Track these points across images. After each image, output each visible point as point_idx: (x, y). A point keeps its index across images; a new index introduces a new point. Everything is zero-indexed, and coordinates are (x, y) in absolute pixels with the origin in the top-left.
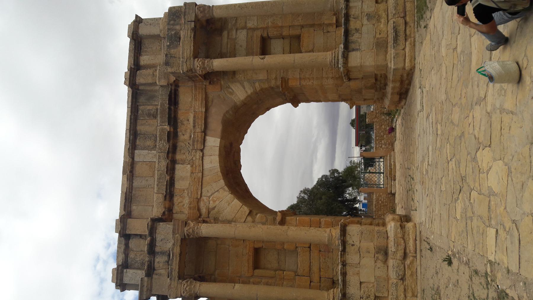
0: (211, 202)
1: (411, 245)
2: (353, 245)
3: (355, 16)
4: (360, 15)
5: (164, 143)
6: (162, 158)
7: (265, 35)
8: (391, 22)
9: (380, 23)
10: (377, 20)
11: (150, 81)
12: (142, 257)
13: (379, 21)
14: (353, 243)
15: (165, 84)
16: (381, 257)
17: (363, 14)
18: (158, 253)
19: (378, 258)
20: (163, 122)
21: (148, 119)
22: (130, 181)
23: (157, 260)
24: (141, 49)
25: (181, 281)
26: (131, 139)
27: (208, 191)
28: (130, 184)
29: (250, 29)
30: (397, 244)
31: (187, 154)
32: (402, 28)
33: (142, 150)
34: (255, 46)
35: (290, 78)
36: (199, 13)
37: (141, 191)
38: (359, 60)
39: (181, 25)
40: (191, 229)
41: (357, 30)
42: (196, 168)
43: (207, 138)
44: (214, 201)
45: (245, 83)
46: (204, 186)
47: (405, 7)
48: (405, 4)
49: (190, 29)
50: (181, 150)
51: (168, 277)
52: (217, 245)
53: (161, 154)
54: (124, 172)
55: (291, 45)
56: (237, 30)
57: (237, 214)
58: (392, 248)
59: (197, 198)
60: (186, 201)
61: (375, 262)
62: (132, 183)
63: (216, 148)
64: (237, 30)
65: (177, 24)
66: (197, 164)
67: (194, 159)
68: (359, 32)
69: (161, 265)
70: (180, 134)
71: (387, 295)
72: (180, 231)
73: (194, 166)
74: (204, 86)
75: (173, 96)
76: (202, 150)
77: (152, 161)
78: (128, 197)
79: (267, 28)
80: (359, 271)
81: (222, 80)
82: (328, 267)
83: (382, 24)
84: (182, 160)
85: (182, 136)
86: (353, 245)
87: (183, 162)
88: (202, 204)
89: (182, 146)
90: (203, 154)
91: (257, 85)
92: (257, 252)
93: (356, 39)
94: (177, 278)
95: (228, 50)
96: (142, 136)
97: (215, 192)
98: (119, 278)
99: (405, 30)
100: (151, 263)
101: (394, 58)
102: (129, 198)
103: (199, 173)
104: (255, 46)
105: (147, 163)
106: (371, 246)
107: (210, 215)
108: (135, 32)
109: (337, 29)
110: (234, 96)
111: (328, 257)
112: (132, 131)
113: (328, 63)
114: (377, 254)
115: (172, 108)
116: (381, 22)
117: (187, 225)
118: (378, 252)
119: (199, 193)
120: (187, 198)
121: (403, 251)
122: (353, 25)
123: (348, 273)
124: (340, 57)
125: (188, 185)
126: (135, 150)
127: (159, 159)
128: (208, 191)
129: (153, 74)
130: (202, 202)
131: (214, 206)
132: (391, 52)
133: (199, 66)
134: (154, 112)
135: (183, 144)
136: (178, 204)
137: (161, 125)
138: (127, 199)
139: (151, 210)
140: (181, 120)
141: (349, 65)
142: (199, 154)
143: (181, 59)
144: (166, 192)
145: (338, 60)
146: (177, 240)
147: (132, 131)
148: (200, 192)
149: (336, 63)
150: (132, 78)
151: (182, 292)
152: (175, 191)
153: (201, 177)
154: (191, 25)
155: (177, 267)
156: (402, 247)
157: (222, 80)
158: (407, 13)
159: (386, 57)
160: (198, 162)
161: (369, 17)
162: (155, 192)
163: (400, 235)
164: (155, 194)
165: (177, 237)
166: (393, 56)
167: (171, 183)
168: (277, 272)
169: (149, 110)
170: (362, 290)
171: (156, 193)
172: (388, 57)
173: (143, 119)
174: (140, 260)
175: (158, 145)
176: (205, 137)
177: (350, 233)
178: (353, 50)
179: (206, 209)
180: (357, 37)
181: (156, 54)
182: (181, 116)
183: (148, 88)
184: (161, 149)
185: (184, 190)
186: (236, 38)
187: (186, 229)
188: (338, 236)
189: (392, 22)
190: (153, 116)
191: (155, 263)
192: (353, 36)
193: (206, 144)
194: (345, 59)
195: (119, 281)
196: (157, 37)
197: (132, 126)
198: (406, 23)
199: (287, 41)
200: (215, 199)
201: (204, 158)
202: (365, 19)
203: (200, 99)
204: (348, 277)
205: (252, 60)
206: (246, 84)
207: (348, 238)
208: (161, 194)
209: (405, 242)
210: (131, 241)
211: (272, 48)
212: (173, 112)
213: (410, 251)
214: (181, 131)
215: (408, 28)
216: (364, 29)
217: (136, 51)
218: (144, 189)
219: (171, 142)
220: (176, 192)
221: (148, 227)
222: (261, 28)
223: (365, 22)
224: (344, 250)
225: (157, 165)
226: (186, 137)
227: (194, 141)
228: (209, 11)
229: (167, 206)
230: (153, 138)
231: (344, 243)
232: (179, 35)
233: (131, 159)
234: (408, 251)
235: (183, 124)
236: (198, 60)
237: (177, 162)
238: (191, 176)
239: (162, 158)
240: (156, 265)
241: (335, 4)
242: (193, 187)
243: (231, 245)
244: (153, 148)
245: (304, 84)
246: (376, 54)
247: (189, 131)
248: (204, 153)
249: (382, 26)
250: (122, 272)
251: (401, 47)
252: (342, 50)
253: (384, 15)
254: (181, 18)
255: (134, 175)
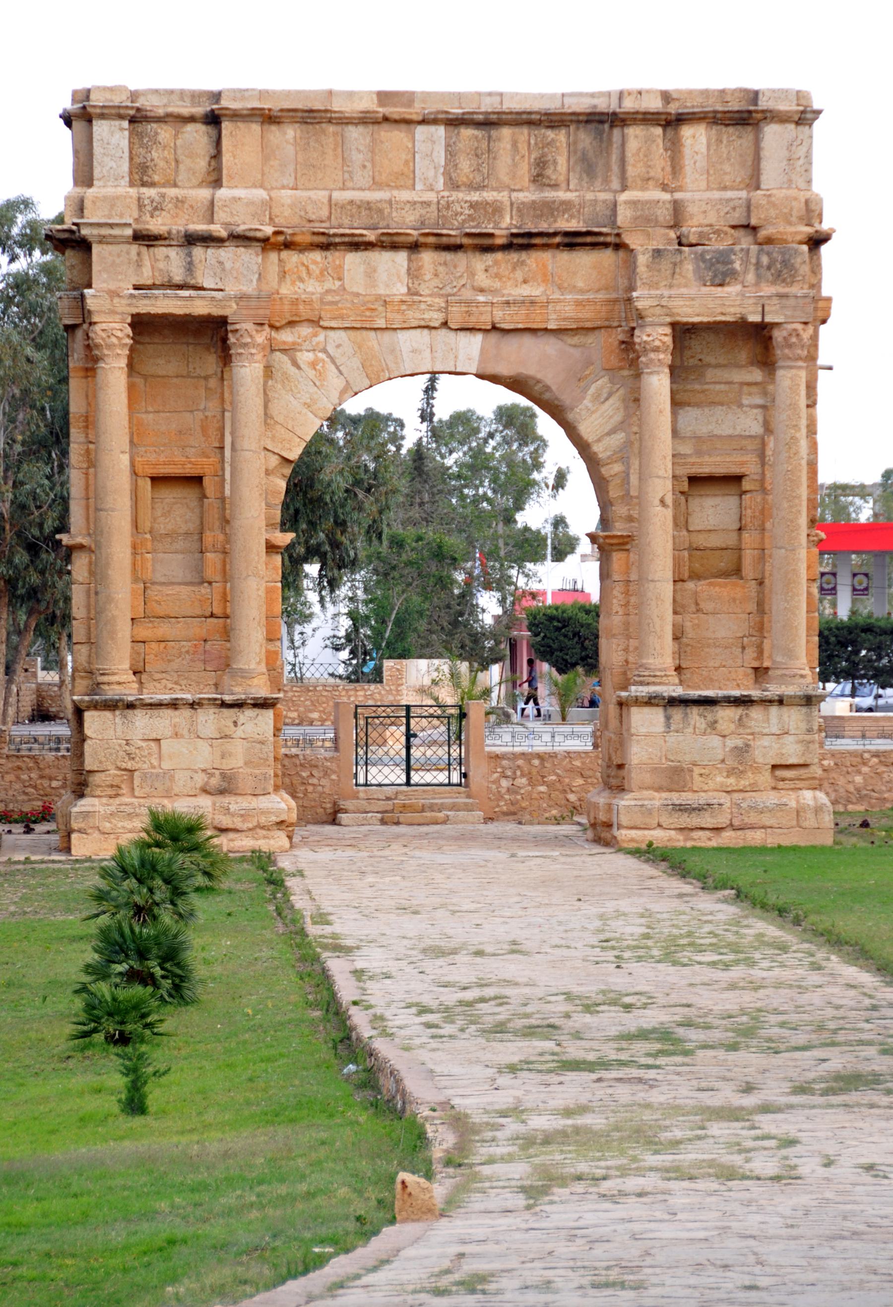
0: (311, 356)
1: (244, 843)
2: (235, 723)
3: (745, 720)
4: (749, 731)
5: (463, 217)
6: (423, 212)
7: (746, 485)
8: (725, 799)
9: (725, 774)
10: (734, 769)
11: (631, 171)
12: (162, 164)
13: (731, 772)
14: (239, 724)
15: (620, 220)
16: (215, 782)
17: (750, 737)
18: (189, 255)
19: (212, 775)
20: (519, 210)
21: (529, 158)
22: (360, 118)
23: (173, 253)
24: (727, 125)
25: (129, 320)
26: (475, 116)
27: (338, 346)
28: (354, 118)
29: (764, 444)
30: (245, 816)
31: (436, 282)
32: (707, 820)
33: (448, 145)
34: (718, 459)
35: (631, 555)
36: (785, 333)
37: (335, 150)
38: (643, 730)
39: (757, 284)
40: (249, 340)
41: (713, 725)
42: (398, 311)
43: (479, 337)
44: (313, 365)
45: (623, 434)
46: (350, 332)
47: (752, 828)
48: (762, 828)
49: (744, 311)
50: (445, 264)
51: (136, 288)
52: (206, 378)
53: (434, 207)
54: (384, 97)
55: (722, 549)
56: (764, 407)
57: (283, 430)
58: (236, 804)
59: (320, 318)
60: (312, 288)
61: (203, 771)
62: (356, 124)
63: (452, 363)
64: (764, 407)
65: (759, 277)
66: (410, 314)
67: (423, 306)
68: (709, 730)
69: (161, 265)
70: (490, 258)
71: (136, 794)
72: (244, 312)
73: (404, 307)
74: (616, 324)
75: (589, 239)
76: (445, 324)
77: (417, 180)
78: (315, 114)
79: (764, 490)
80: (182, 736)
81: (632, 372)
82: (169, 661)
83: (722, 779)
84: (420, 268)
85: (483, 267)
86: (235, 723)
87: (413, 273)
88: (305, 330)
89: (455, 267)
90: (435, 328)
91: (617, 468)
92: (196, 480)
93: (693, 723)
94: (135, 311)
95: (711, 387)
96: (484, 145)
97: (337, 368)
98: (106, 111)
99: (702, 829)
100: (165, 239)
101: (642, 806)
102: (315, 118)
103: (383, 321)
104: (718, 459)
105: (411, 164)
106: (236, 762)
107: (278, 353)
108: (768, 115)
109: (750, 671)
110: (590, 405)
111: (192, 660)
112: (495, 116)
113: (644, 661)
114: (221, 774)
115: (558, 239)
116: (728, 777)
117: (259, 328)
118: (224, 776)
119: (333, 324)
120: (319, 290)
121: (231, 826)
122: (726, 715)
123: (177, 713)
124: (652, 689)
125: (355, 290)
126: (446, 124)
127: (422, 203)
128: (338, 346)
129: (649, 179)
130: (310, 330)
131: (302, 366)
132: (657, 799)
133: (651, 338)
134: (548, 177)
135: (461, 268)
136: (303, 264)
137: (512, 204)
138: (311, 115)
139: (285, 182)
140: (524, 261)
141: (634, 710)
142: (436, 318)
143: (666, 293)
144: (335, 235)
145: (648, 684)
146: (223, 307)
147: (495, 116)
148: (335, 326)
149: (642, 679)
150: (640, 116)
151: (104, 326)
152: (337, 254)
153: (376, 326)
154: (754, 313)
155: (160, 311)
156: (238, 823)
157: (632, 372)
158: (739, 833)
159: (647, 788)
160: (414, 316)
161: (742, 751)
162: (336, 195)
163: (263, 820)
164: (326, 193)
165: (230, 307)
166: (646, 803)
167: (357, 245)
168: (148, 536)
169: (555, 162)
170: (144, 744)
171: (330, 197)
172: (646, 793)
173: (529, 144)
174: (152, 160)
175: (461, 195)
176: (480, 330)
177: (260, 718)
178: (668, 718)
179: (294, 343)
180: (698, 725)
181: (711, 172)
182: (534, 259)
183: (615, 157)
184: (448, 206)
185: (340, 279)
186: (741, 406)
187: (249, 326)
188: (253, 691)
189: (722, 801)
190: (538, 175)
191: (164, 249)
192: (700, 715)
193: (461, 334)
194: (646, 700)
195: (98, 111)
196: (754, 181)
197: (509, 117)
198: (717, 830)
199: (731, 540)
200: (318, 367)
201: (426, 331)
202: (739, 743)
203: (580, 315)
204: (168, 712)
205: (659, 477)
206: (620, 437)
207: (250, 713)
208: (327, 213)
209: (250, 830)
210: (202, 128)
211: (717, 500)
212: (545, 240)
213: (232, 840)
214: (496, 263)
215: (708, 833)
216: (715, 741)
217: (719, 116)
218: (340, 160)
219: (466, 241)
220: (333, 256)
221: (251, 230)
222: (763, 474)
223: (731, 743)
224: (224, 705)
225: (405, 195)
226: (482, 279)
227: (468, 303)
228: (789, 358)
229: (298, 239)
230: (479, 179)
231: (238, 705)
232: (728, 284)
233: (420, 118)
234: (231, 835)
235: (514, 269)
236: (666, 335)
237: (413, 257)
238: (378, 297)
239: (423, 212)
240: (161, 251)
241: (779, 672)
242: (349, 305)
243: (207, 414)
244: (451, 179)
245: (615, 592)
246: (656, 768)
247: (497, 284)
248: (439, 331)
249: (719, 779)
250: (121, 117)
251: (665, 820)
252: (665, 694)
253: (743, 783)
254: (773, 283)
255: (376, 127)
